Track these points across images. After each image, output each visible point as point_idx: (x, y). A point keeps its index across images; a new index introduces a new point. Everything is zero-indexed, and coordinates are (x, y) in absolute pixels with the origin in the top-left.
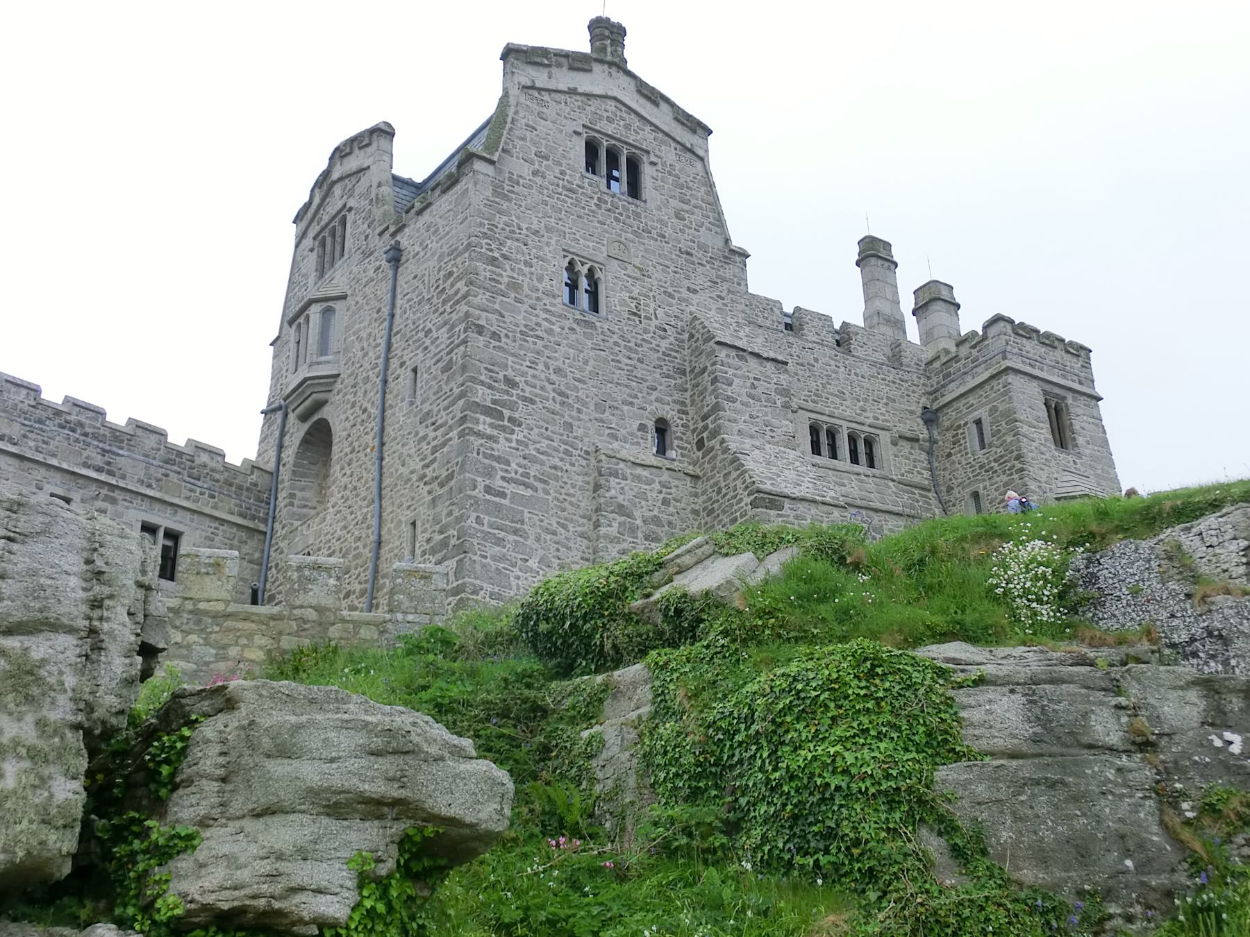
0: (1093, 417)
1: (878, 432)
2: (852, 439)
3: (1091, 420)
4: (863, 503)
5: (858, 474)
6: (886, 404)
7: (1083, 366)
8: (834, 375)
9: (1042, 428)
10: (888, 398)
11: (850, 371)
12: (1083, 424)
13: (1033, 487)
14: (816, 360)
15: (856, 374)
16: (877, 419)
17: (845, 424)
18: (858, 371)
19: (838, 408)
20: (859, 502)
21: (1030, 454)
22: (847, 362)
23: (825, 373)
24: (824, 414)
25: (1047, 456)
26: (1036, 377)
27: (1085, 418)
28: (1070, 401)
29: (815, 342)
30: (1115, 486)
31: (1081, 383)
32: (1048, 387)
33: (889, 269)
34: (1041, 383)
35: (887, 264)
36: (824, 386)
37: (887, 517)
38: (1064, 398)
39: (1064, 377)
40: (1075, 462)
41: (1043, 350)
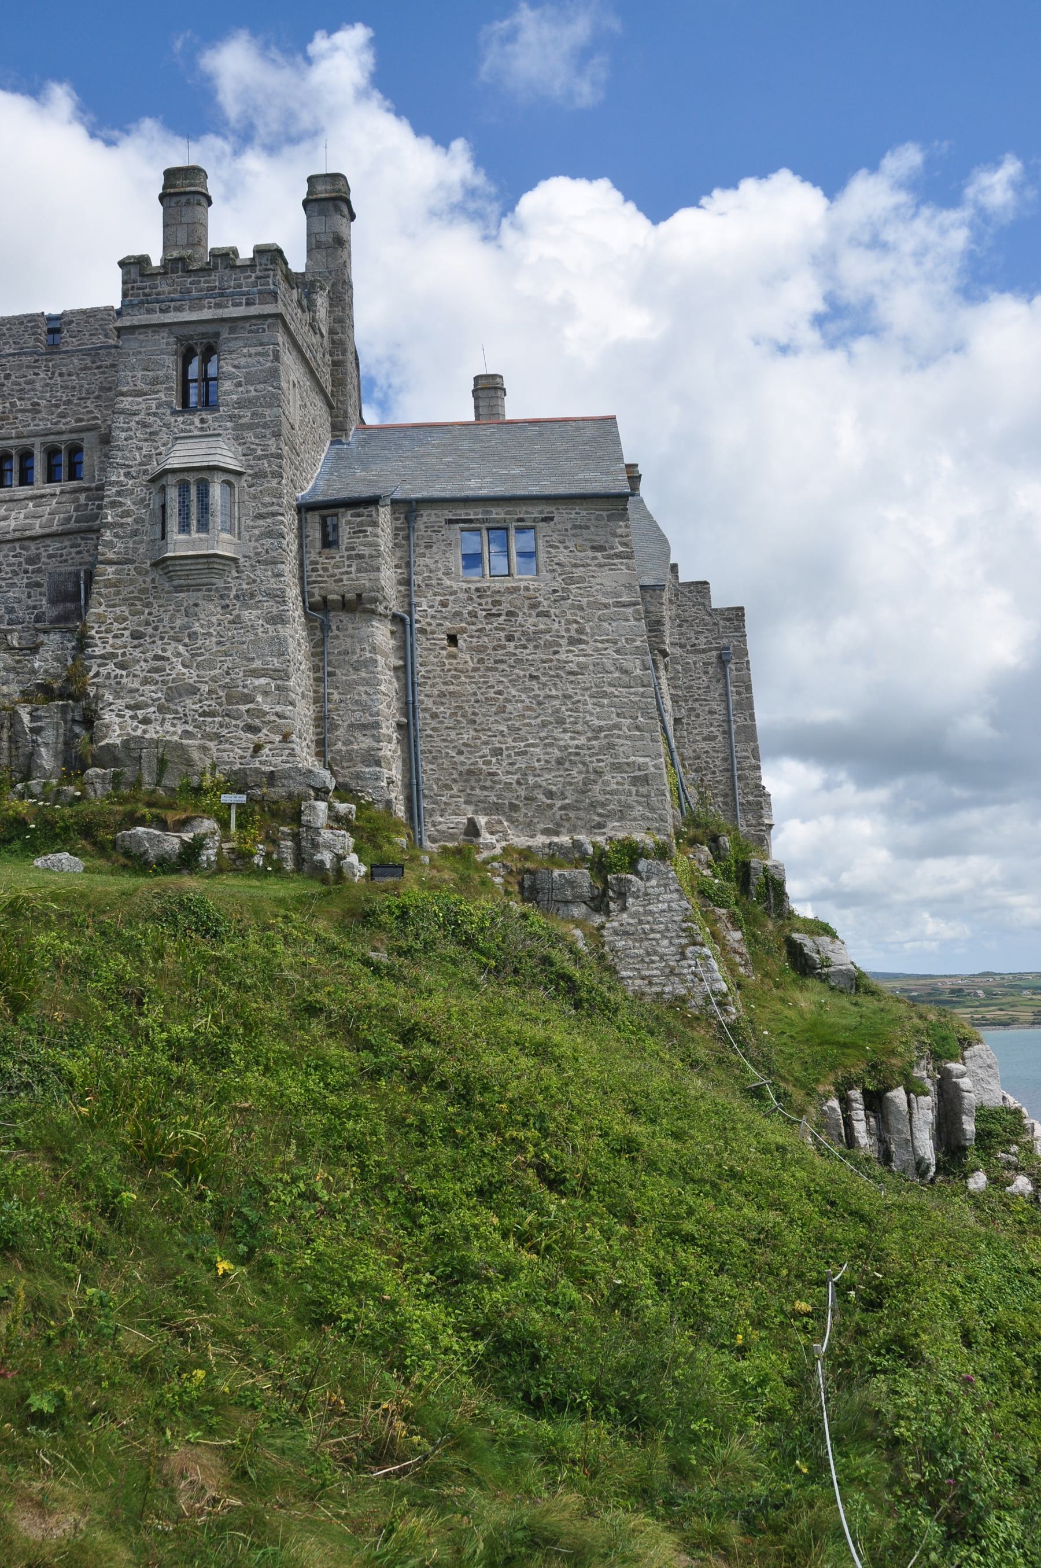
0: (261, 344)
1: (82, 435)
2: (52, 452)
3: (253, 350)
4: (17, 534)
5: (43, 496)
6: (98, 397)
7: (257, 278)
8: (28, 387)
9: (156, 393)
10: (102, 389)
11: (53, 373)
12: (236, 363)
13: (114, 478)
14: (7, 377)
15: (61, 375)
16: (80, 420)
17: (37, 441)
18: (64, 370)
19: (29, 425)
20: (9, 537)
21: (123, 435)
22: (50, 364)
23: (17, 387)
24: (12, 438)
25: (155, 428)
26: (164, 325)
27: (245, 351)
28: (225, 335)
29: (10, 355)
30: (268, 432)
31: (249, 304)
32: (186, 331)
33: (188, 203)
34: (175, 329)
35: (183, 199)
36: (13, 404)
37: (48, 542)
38: (217, 335)
39: (218, 306)
40: (202, 421)
41: (189, 280)
